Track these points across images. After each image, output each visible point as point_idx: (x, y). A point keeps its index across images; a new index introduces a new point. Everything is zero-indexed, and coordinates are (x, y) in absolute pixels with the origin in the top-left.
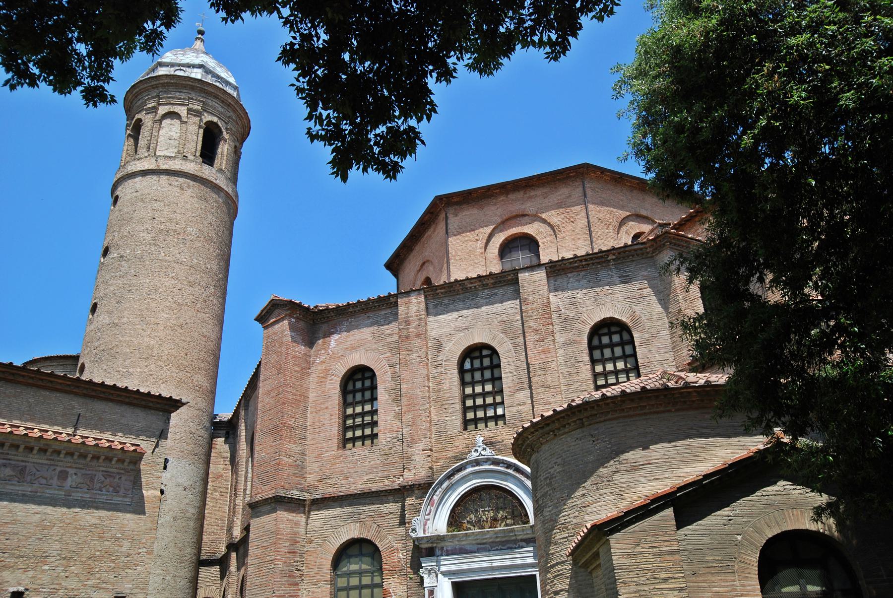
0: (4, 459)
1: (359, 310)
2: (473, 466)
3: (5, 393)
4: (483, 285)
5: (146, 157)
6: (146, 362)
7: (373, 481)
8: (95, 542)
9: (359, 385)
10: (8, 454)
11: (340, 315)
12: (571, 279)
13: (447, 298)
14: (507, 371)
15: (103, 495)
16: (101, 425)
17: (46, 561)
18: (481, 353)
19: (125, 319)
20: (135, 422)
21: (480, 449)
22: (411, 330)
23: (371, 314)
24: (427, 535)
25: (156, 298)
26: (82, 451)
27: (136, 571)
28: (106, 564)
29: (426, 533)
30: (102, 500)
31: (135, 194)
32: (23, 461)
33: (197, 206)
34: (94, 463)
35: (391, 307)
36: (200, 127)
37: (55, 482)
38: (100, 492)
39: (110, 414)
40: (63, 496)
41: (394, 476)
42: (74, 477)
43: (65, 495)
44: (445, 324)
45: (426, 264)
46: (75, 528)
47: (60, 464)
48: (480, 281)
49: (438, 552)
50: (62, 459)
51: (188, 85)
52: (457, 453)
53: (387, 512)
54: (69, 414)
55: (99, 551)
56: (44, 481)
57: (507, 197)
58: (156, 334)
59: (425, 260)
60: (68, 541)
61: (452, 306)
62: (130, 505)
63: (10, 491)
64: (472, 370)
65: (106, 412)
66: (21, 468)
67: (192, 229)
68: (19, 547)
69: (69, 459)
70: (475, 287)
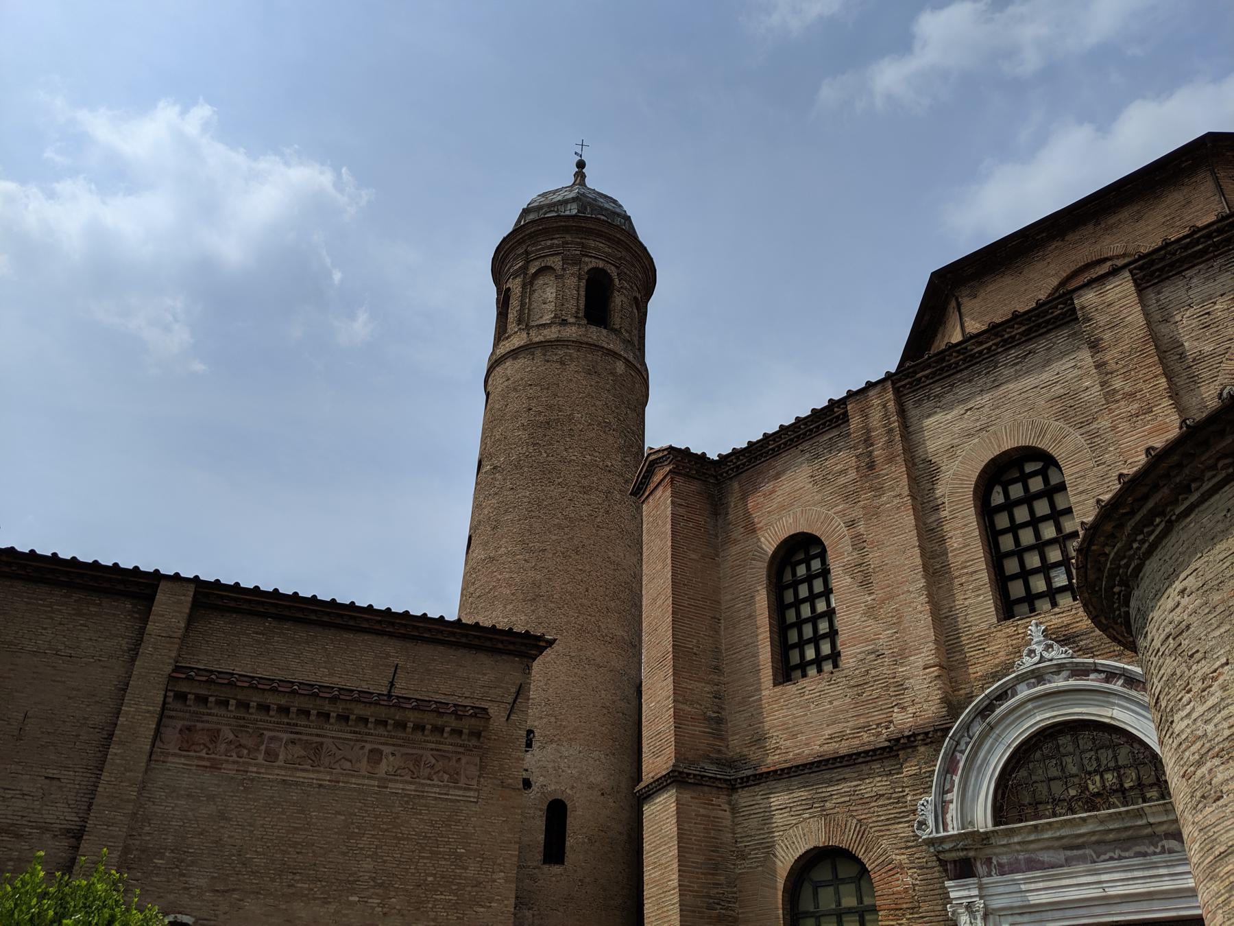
0: (291, 733)
1: (785, 444)
2: (1030, 686)
3: (293, 638)
4: (1005, 341)
5: (517, 332)
6: (532, 606)
7: (842, 737)
8: (425, 861)
9: (801, 570)
10: (297, 725)
11: (756, 458)
12: (1194, 280)
13: (937, 385)
14: (1081, 489)
15: (434, 786)
16: (429, 680)
17: (354, 889)
18: (1022, 470)
19: (503, 549)
20: (478, 673)
21: (1039, 649)
23: (806, 446)
24: (951, 832)
25: (540, 515)
26: (397, 718)
27: (490, 910)
28: (443, 897)
29: (950, 828)
30: (433, 795)
31: (506, 383)
32: (318, 735)
33: (585, 383)
34: (419, 736)
35: (839, 425)
36: (580, 279)
37: (364, 766)
38: (429, 782)
39: (442, 663)
40: (376, 788)
41: (878, 725)
42: (391, 758)
43: (378, 787)
44: (939, 430)
46: (395, 838)
47: (369, 738)
48: (997, 335)
49: (981, 869)
50: (372, 731)
51: (559, 227)
52: (997, 665)
53: (873, 794)
54: (382, 666)
55: (432, 875)
56: (347, 765)
57: (1063, 240)
58: (543, 565)
60: (385, 858)
61: (949, 397)
62: (477, 802)
63: (302, 780)
64: (1009, 506)
65: (435, 660)
66: (314, 745)
67: (580, 415)
68: (315, 865)
69: (381, 730)
70: (989, 349)
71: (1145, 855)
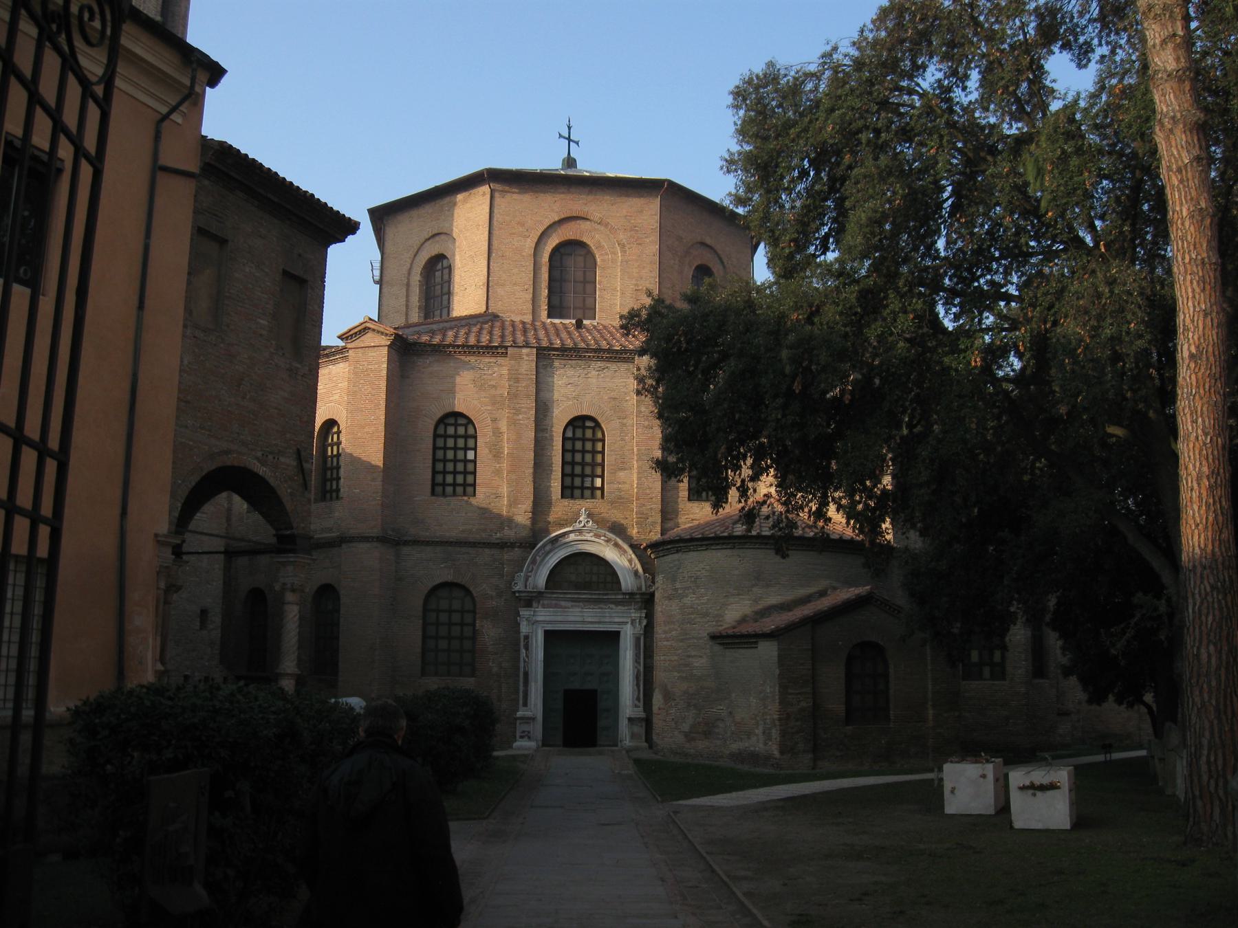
9: (451, 430)
22: (520, 388)
41: (491, 531)
45: (443, 237)
49: (535, 604)
59: (445, 231)
71: (602, 608)
